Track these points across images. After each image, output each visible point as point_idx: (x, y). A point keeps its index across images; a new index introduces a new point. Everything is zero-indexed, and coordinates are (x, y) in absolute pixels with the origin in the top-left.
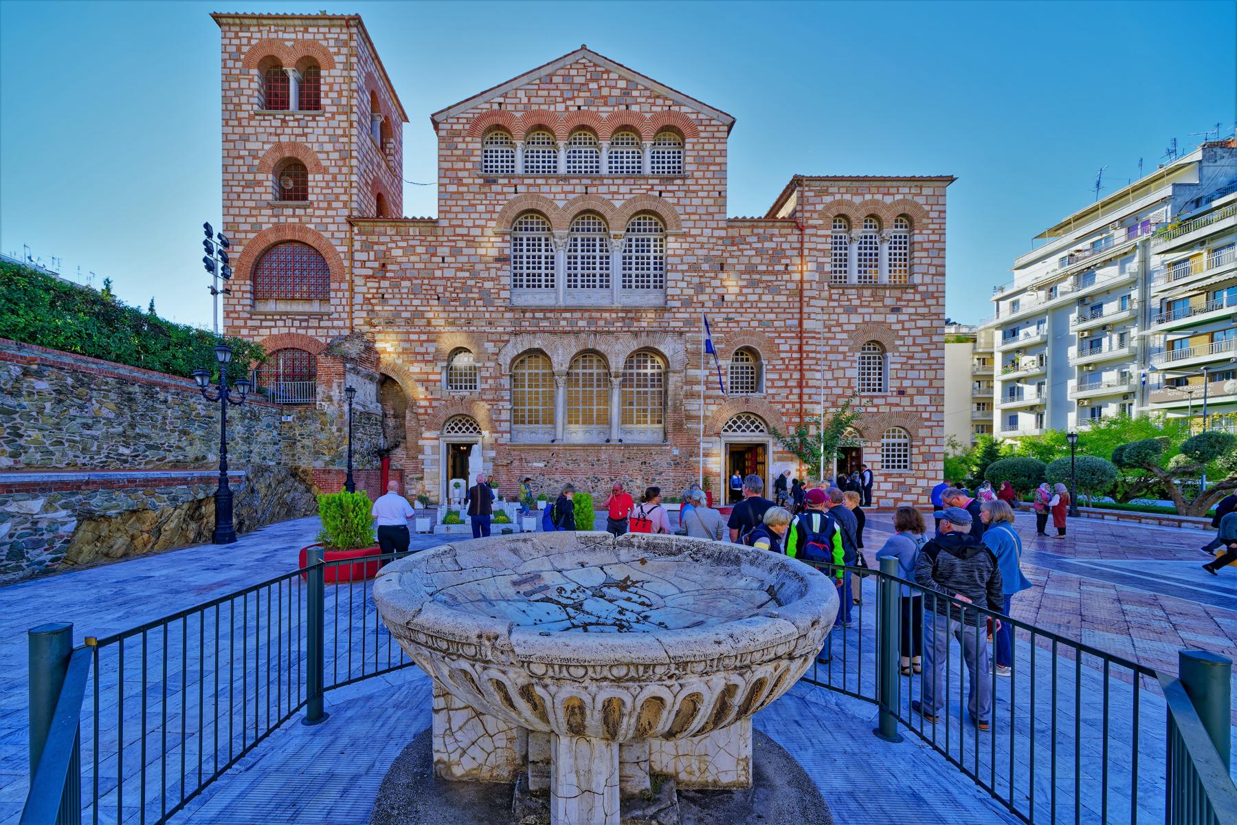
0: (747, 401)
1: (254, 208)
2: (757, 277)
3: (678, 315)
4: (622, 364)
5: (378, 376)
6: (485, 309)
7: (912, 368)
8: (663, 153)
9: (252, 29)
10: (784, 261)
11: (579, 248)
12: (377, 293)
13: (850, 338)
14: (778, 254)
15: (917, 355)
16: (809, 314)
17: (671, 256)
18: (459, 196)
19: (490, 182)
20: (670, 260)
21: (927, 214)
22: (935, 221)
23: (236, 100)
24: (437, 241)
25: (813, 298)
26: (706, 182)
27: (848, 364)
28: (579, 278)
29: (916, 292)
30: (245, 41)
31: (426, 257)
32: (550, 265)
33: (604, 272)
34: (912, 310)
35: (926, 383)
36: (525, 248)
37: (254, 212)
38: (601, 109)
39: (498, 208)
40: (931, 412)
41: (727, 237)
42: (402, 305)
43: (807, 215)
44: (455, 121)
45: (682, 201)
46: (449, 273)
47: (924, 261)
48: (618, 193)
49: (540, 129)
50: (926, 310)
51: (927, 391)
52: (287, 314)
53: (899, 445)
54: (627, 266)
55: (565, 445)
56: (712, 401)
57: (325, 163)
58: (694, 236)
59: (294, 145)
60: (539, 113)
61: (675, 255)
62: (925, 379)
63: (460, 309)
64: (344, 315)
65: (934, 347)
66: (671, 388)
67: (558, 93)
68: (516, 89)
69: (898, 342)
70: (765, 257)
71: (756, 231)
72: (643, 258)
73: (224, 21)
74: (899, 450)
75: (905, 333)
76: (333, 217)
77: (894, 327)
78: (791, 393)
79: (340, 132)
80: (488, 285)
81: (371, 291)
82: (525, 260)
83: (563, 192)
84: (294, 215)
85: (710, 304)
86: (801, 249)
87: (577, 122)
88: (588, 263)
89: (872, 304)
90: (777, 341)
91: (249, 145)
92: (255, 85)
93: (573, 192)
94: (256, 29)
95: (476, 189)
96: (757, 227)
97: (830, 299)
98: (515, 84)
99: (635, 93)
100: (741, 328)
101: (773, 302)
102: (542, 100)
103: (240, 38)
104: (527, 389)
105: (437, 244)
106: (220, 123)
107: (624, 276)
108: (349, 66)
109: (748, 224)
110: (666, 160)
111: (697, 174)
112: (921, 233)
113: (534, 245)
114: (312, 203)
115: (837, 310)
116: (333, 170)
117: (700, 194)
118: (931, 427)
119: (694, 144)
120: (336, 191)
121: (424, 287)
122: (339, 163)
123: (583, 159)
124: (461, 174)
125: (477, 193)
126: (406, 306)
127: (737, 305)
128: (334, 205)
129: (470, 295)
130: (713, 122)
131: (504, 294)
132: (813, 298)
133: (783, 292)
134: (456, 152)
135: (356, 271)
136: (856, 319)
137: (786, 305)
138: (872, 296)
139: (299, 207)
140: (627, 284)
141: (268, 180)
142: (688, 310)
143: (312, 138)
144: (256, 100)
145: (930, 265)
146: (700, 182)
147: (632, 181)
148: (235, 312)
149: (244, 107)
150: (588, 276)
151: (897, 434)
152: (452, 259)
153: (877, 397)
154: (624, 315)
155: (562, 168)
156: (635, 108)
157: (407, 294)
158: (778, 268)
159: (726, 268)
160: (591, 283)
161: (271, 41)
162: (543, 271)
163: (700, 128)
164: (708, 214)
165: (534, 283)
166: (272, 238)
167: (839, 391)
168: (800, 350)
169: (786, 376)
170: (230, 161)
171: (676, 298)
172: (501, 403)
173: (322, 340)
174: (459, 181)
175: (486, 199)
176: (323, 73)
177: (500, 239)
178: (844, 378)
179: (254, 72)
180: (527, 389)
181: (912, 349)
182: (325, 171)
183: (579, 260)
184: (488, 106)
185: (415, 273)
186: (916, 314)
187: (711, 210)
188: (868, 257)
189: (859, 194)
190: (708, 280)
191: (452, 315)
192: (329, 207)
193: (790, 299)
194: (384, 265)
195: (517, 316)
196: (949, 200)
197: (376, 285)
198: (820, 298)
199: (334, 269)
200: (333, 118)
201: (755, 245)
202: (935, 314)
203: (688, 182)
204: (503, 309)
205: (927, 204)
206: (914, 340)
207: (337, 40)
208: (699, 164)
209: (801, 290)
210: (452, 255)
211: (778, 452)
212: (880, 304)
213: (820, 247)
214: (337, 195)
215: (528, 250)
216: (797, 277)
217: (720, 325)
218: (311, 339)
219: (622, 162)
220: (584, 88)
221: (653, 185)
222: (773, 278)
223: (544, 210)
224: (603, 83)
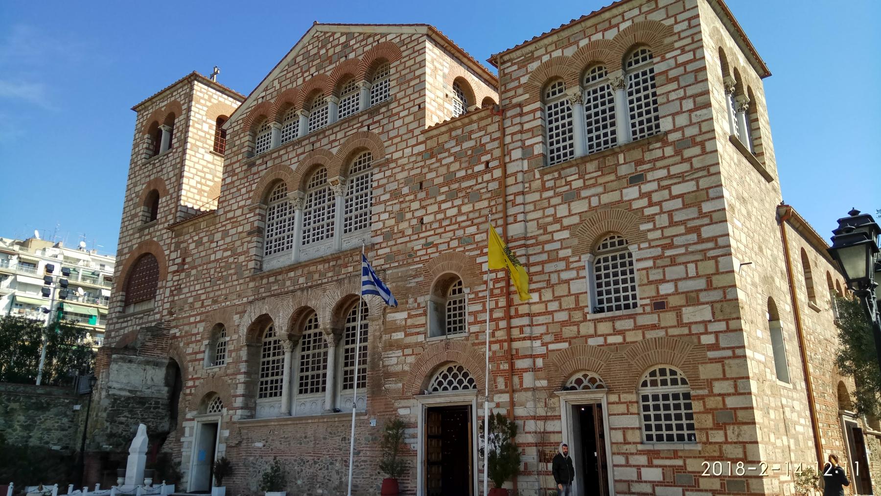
0: (447, 345)
2: (455, 186)
3: (380, 252)
5: (166, 361)
7: (673, 261)
10: (484, 158)
13: (573, 235)
15: (677, 241)
16: (515, 216)
18: (231, 186)
19: (252, 165)
21: (669, 31)
25: (523, 193)
26: (407, 99)
27: (573, 274)
29: (665, 143)
34: (663, 173)
37: (132, 237)
38: (327, 69)
39: (254, 187)
40: (717, 334)
41: (426, 150)
46: (219, 255)
48: (335, 141)
50: (685, 167)
51: (703, 297)
53: (676, 396)
57: (168, 187)
59: (156, 179)
61: (379, 187)
62: (698, 276)
63: (222, 286)
65: (706, 220)
69: (643, 227)
70: (463, 160)
71: (454, 134)
73: (138, 109)
74: (677, 407)
75: (655, 210)
77: (636, 205)
78: (497, 328)
79: (178, 160)
87: (310, 89)
89: (600, 181)
90: (479, 260)
91: (137, 189)
95: (241, 175)
96: (455, 128)
97: (544, 189)
98: (271, 78)
106: (127, 178)
109: (443, 129)
111: (399, 96)
112: (664, 59)
115: (554, 201)
117: (402, 114)
118: (721, 360)
119: (396, 66)
131: (252, 265)
132: (523, 193)
134: (235, 149)
136: (579, 206)
138: (599, 169)
141: (141, 210)
142: (390, 243)
143: (165, 171)
145: (681, 99)
147: (347, 124)
151: (668, 377)
154: (334, 263)
156: (352, 56)
158: (478, 168)
161: (156, 112)
164: (409, 131)
166: (136, 255)
167: (562, 316)
172: (239, 377)
176: (176, 121)
177: (252, 214)
178: (569, 294)
179: (146, 136)
184: (255, 103)
186: (670, 177)
187: (411, 127)
189: (571, 45)
191: (217, 294)
192: (166, 221)
193: (493, 203)
194: (184, 260)
195: (257, 284)
199: (161, 271)
200: (176, 152)
201: (453, 151)
203: (392, 106)
204: (248, 280)
205: (668, 17)
206: (671, 217)
209: (504, 186)
212: (612, 177)
213: (526, 126)
216: (498, 173)
217: (419, 253)
220: (317, 56)
221: (362, 122)
222: (472, 182)
224: (329, 46)
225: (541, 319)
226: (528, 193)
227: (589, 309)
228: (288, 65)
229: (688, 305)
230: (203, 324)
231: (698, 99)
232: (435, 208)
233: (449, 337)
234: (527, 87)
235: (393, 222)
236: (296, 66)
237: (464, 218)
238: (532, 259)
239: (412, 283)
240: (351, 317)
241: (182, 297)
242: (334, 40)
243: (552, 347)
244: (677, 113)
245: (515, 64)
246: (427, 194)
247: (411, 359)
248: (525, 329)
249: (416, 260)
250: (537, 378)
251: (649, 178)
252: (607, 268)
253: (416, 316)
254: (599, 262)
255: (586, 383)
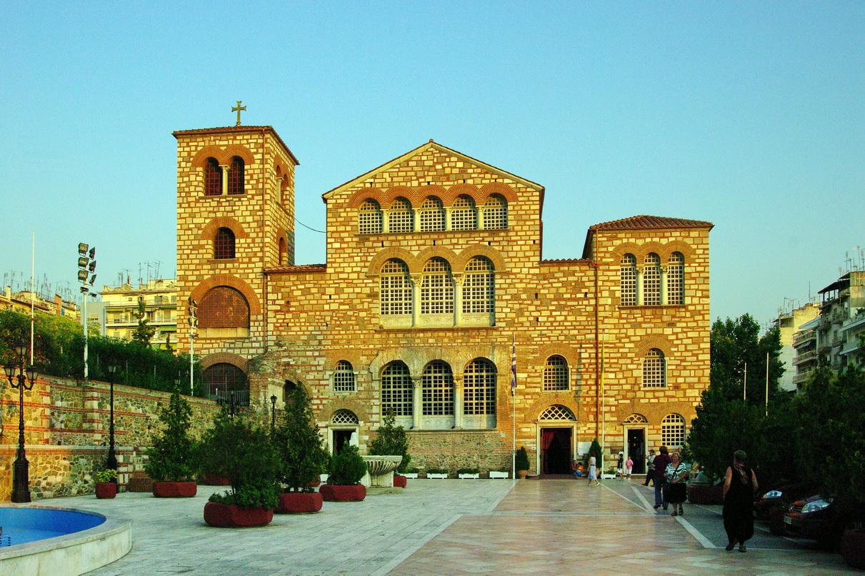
0: (557, 396)
1: (198, 264)
2: (563, 303)
3: (503, 333)
4: (461, 371)
5: (284, 383)
6: (360, 332)
7: (685, 368)
8: (493, 210)
9: (198, 140)
10: (584, 291)
11: (430, 283)
12: (283, 323)
13: (636, 346)
14: (579, 285)
15: (688, 359)
16: (603, 330)
17: (498, 289)
18: (342, 251)
20: (497, 292)
22: (700, 256)
23: (187, 190)
24: (325, 284)
26: (524, 233)
27: (635, 366)
28: (430, 306)
29: (687, 311)
30: (193, 148)
31: (318, 296)
32: (408, 297)
33: (449, 300)
34: (684, 325)
35: (696, 380)
36: (390, 284)
37: (198, 267)
38: (444, 183)
39: (370, 259)
42: (301, 331)
43: (603, 255)
44: (339, 197)
45: (505, 248)
46: (334, 306)
47: (693, 287)
48: (457, 244)
49: (403, 200)
50: (695, 324)
52: (221, 339)
54: (466, 296)
55: (419, 431)
56: (530, 397)
57: (247, 230)
58: (515, 274)
59: (226, 219)
60: (400, 188)
61: (501, 289)
63: (342, 332)
64: (260, 339)
65: (701, 352)
66: (498, 387)
67: (413, 173)
68: (383, 172)
69: (673, 349)
71: (562, 268)
72: (478, 289)
76: (252, 268)
78: (590, 390)
80: (363, 314)
81: (280, 321)
82: (390, 293)
83: (417, 245)
84: (225, 269)
85: (528, 324)
86: (596, 281)
88: (437, 294)
89: (653, 321)
91: (196, 221)
92: (199, 179)
93: (424, 245)
94: (201, 139)
95: (354, 245)
97: (620, 318)
99: (470, 171)
100: (552, 341)
101: (576, 321)
102: (401, 179)
103: (190, 146)
104: (392, 389)
105: (326, 286)
107: (464, 303)
108: (263, 161)
110: (495, 216)
111: (516, 228)
112: (690, 266)
113: (396, 282)
114: (238, 260)
116: (253, 235)
117: (519, 243)
119: (514, 206)
120: (255, 250)
121: (317, 317)
122: (258, 230)
123: (433, 218)
124: (343, 235)
125: (355, 248)
126: (303, 331)
127: (549, 324)
128: (253, 260)
129: (349, 322)
130: (528, 190)
133: (583, 314)
134: (339, 219)
135: (270, 308)
136: (640, 332)
137: (586, 323)
138: (653, 315)
139: (229, 263)
140: (466, 309)
141: (209, 245)
142: (512, 329)
143: (239, 213)
144: (201, 189)
145: (696, 290)
146: (519, 234)
147: (468, 235)
148: (185, 338)
149: (193, 194)
150: (437, 304)
152: (337, 297)
153: (658, 391)
155: (418, 228)
156: (470, 182)
157: (305, 322)
159: (539, 297)
160: (439, 310)
161: (210, 147)
162: (403, 301)
163: (518, 194)
165: (397, 310)
166: (211, 285)
167: (628, 387)
168: (597, 357)
169: (586, 376)
170: (182, 232)
171: (502, 320)
172: (373, 401)
173: (244, 357)
174: (342, 241)
175: (361, 252)
176: (246, 167)
177: (371, 281)
178: (632, 377)
180: (392, 389)
181: (685, 354)
182: (247, 236)
183: (430, 292)
184: (362, 185)
185: (310, 308)
186: (687, 327)
187: (527, 254)
188: (652, 284)
189: (641, 238)
190: (526, 306)
191: (336, 337)
192: (250, 262)
193: (589, 319)
194: (288, 302)
195: (383, 337)
196: (710, 240)
197: (283, 317)
198: (612, 317)
199: (253, 306)
200: (253, 198)
201: (561, 279)
202: (702, 327)
203: (511, 234)
206: (686, 347)
207: (255, 143)
208: (518, 221)
209: (596, 311)
210: (336, 294)
211: (581, 434)
212: (660, 321)
213: (611, 278)
214: (256, 253)
215: (392, 286)
216: (593, 302)
217: (535, 339)
218: (237, 356)
219: (462, 219)
220: (433, 169)
221: (483, 237)
222: (576, 303)
223: (403, 259)
224: (446, 165)
225: (616, 387)
226: (610, 318)
227: (642, 385)
228: (400, 164)
229: (689, 389)
230: (325, 359)
231: (704, 293)
232: (548, 313)
233: (558, 391)
234: (613, 254)
235: (514, 315)
236: (409, 169)
237: (570, 324)
238: (612, 355)
239: (531, 357)
240: (468, 369)
241: (290, 333)
242: (450, 161)
243: (620, 402)
244: (694, 297)
245: (605, 237)
246: (541, 303)
247: (531, 402)
248: (607, 392)
249: (533, 343)
250: (613, 416)
251: (678, 326)
252: (649, 365)
253: (534, 377)
254: (645, 361)
255: (635, 419)
